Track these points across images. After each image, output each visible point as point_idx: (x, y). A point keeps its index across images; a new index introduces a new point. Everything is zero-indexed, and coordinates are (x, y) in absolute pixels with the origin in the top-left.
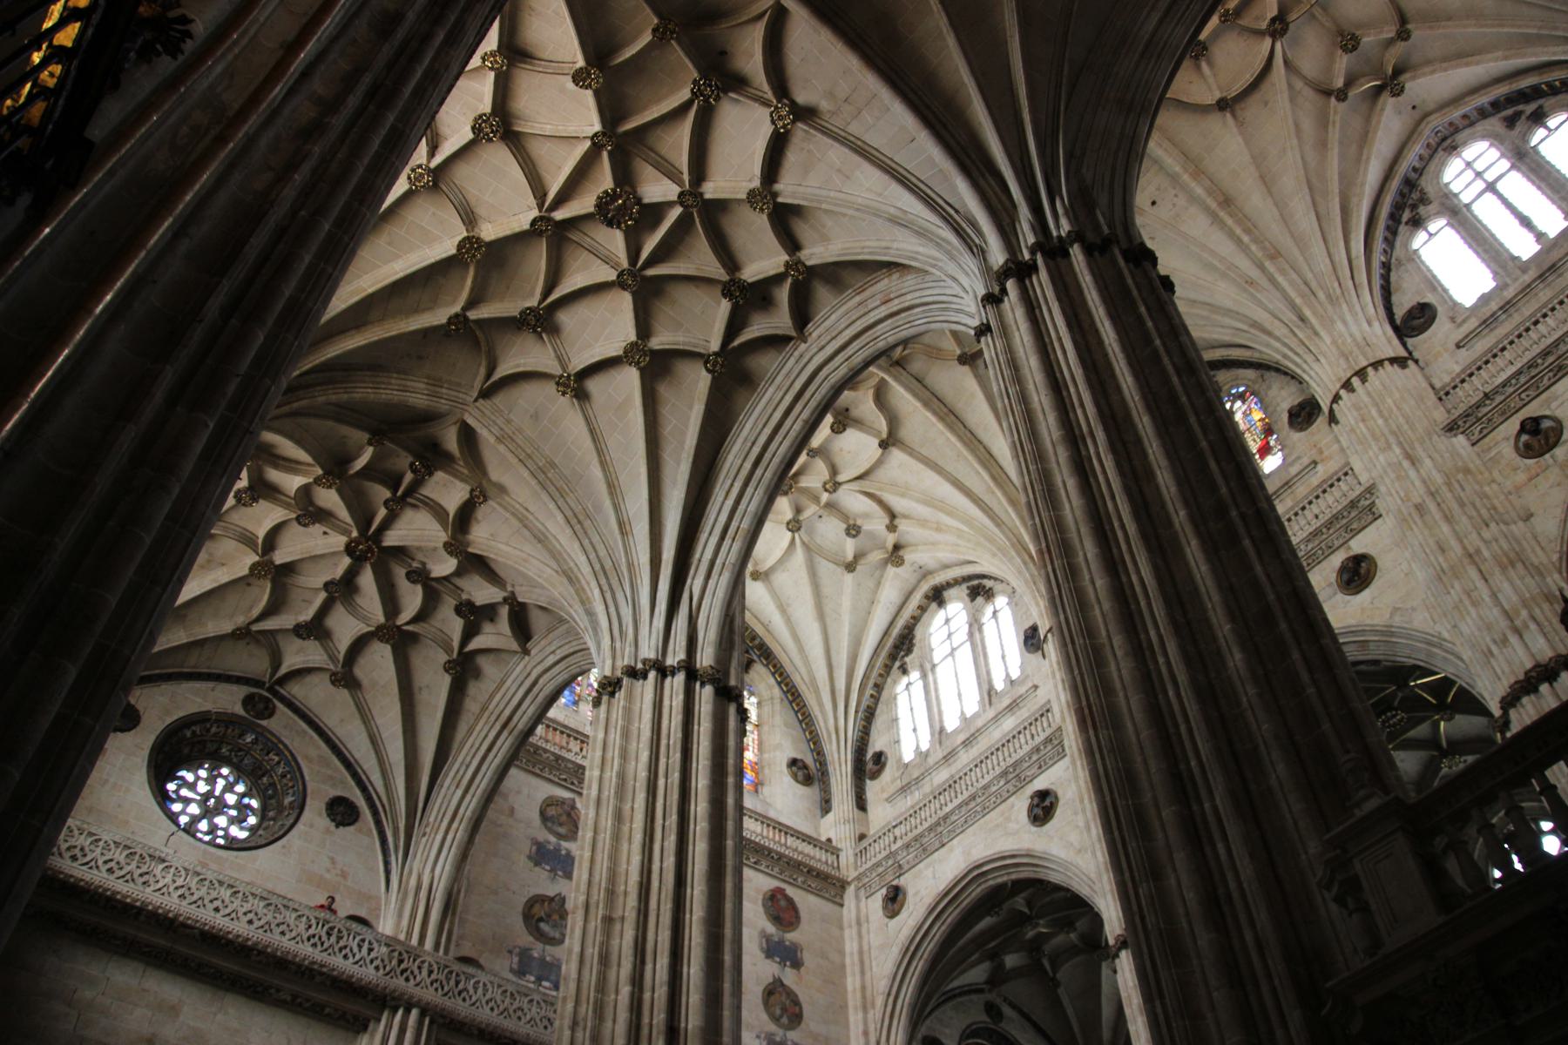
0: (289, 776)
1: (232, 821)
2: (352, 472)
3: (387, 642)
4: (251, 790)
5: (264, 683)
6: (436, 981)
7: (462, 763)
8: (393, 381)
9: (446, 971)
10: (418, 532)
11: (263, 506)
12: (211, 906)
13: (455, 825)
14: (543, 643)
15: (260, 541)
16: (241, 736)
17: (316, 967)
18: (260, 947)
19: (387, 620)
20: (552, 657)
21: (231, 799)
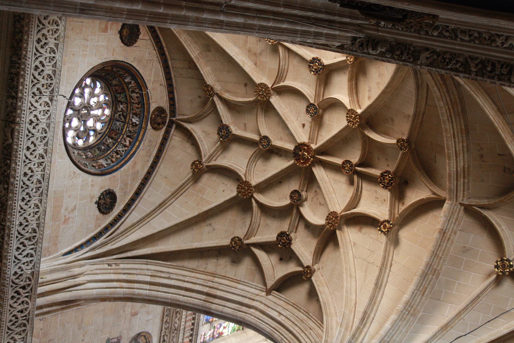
0: (119, 156)
1: (77, 129)
2: (366, 133)
3: (239, 192)
4: (99, 133)
5: (174, 116)
6: (17, 318)
7: (168, 273)
8: (461, 144)
9: (25, 322)
10: (331, 190)
11: (312, 78)
12: (29, 144)
13: (124, 285)
14: (281, 303)
15: (282, 84)
16: (136, 114)
17: (7, 232)
18: (11, 188)
19: (255, 187)
20: (276, 313)
21: (90, 123)
